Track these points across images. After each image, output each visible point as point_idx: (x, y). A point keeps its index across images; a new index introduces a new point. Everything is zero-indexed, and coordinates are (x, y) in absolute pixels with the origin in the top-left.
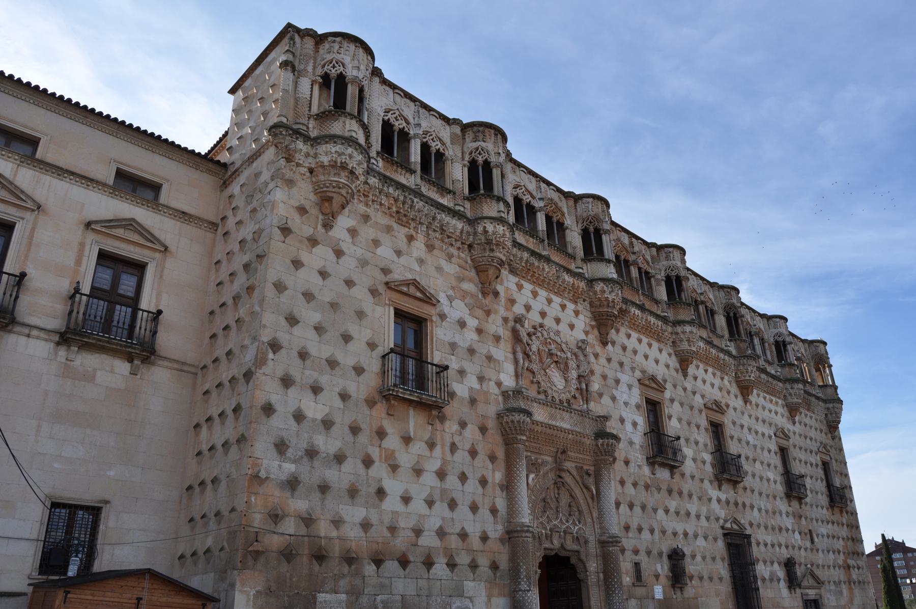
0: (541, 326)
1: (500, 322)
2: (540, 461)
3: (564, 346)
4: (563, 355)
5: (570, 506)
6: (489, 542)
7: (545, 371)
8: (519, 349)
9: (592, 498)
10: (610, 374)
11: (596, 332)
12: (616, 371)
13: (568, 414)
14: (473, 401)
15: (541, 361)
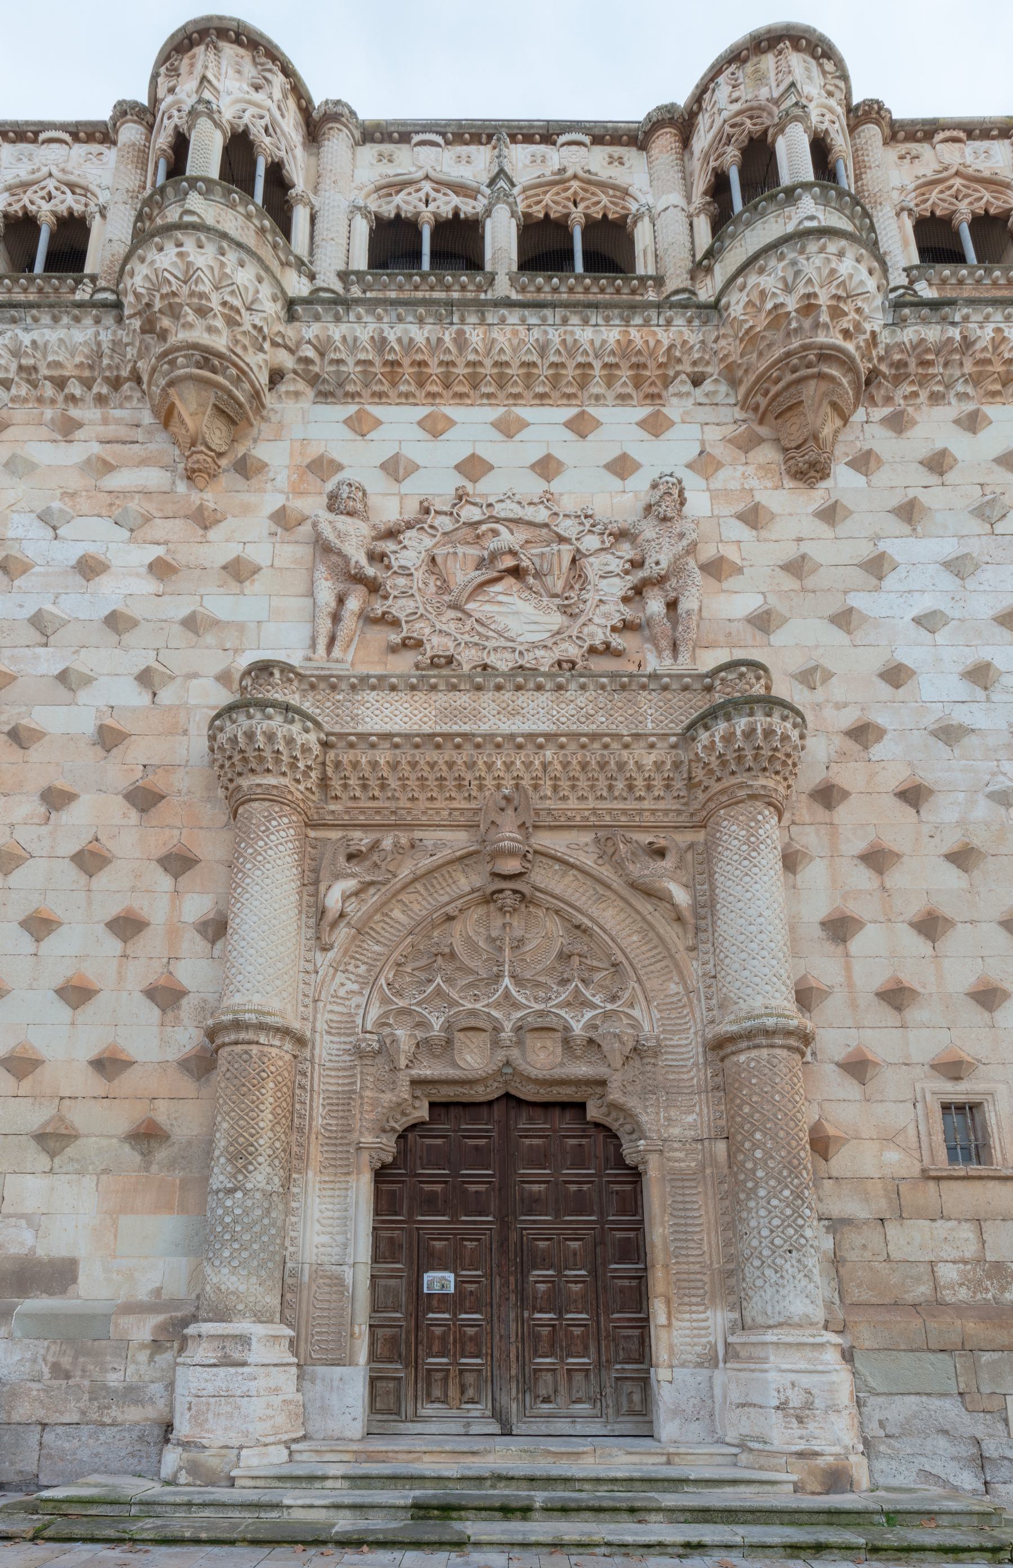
0: (461, 497)
1: (259, 525)
2: (387, 843)
3: (567, 527)
4: (565, 547)
5: (565, 957)
6: (128, 1082)
7: (455, 606)
8: (321, 571)
9: (679, 919)
10: (833, 551)
11: (767, 454)
12: (875, 539)
13: (544, 698)
14: (109, 738)
15: (444, 588)
